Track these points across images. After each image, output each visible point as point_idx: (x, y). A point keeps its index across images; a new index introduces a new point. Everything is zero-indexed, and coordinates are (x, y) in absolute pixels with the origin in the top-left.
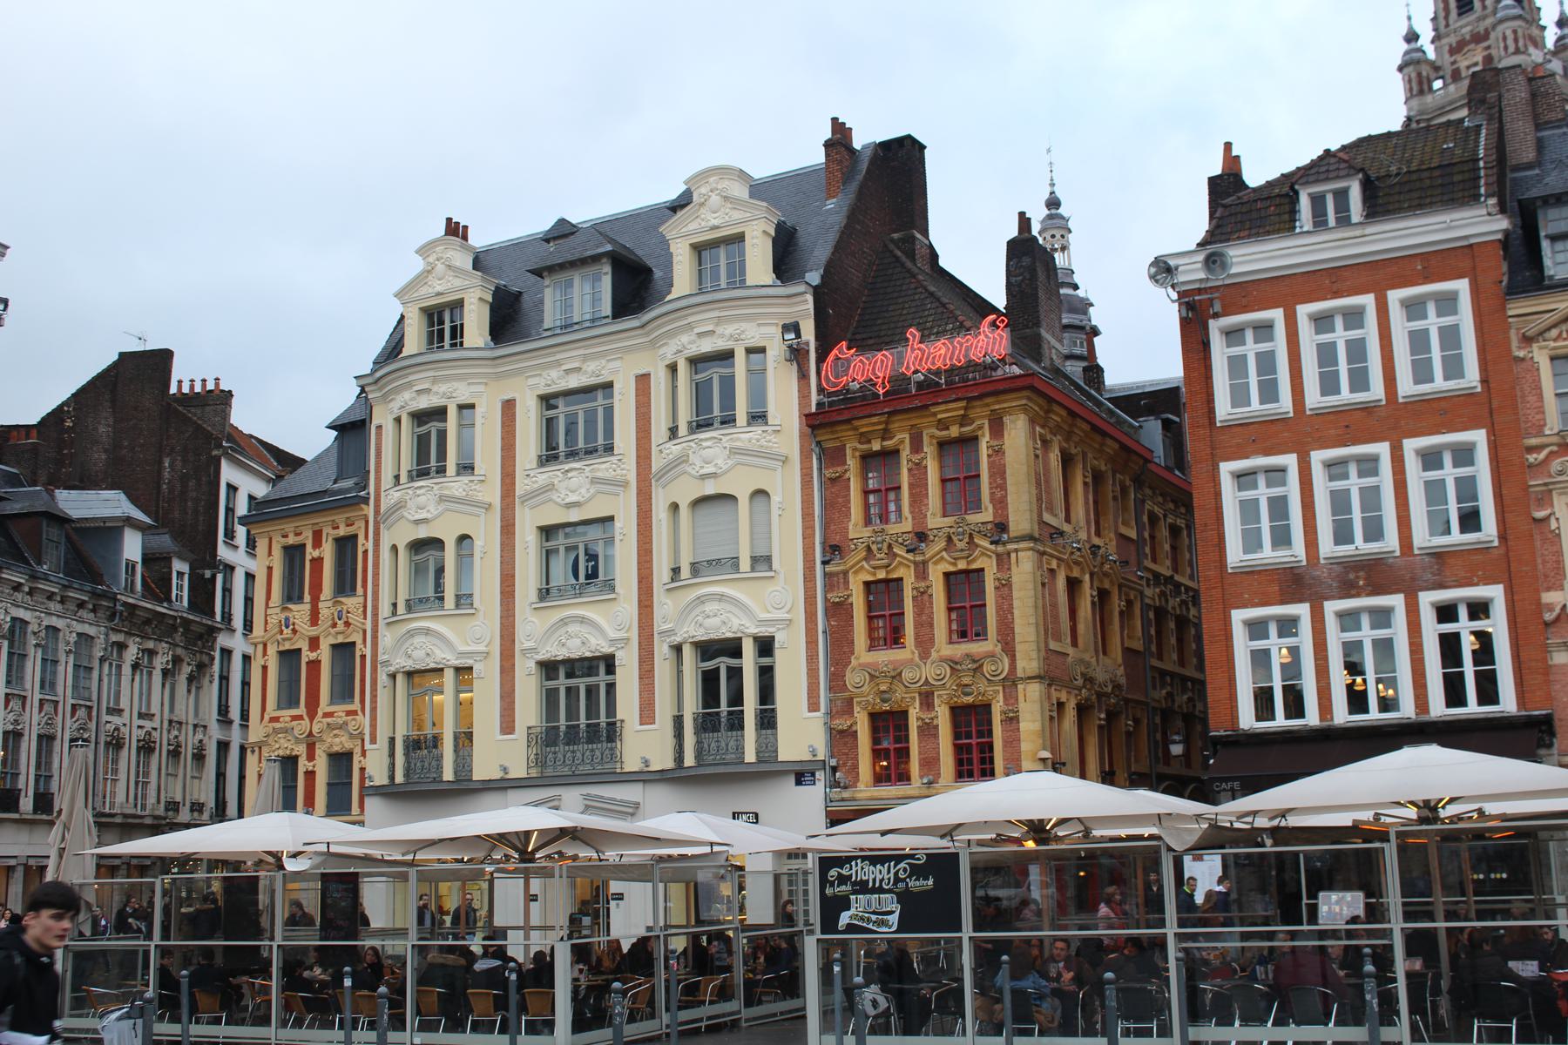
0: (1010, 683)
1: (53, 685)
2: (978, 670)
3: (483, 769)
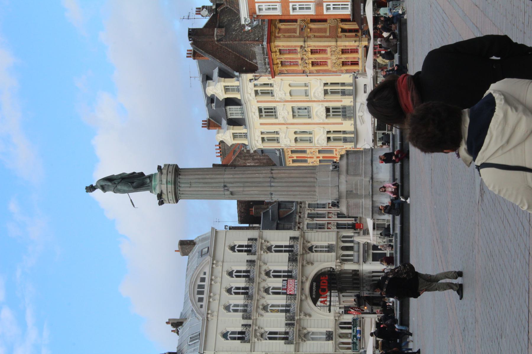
0: (337, 46)
1: (324, 205)
2: (334, 51)
3: (352, 129)
